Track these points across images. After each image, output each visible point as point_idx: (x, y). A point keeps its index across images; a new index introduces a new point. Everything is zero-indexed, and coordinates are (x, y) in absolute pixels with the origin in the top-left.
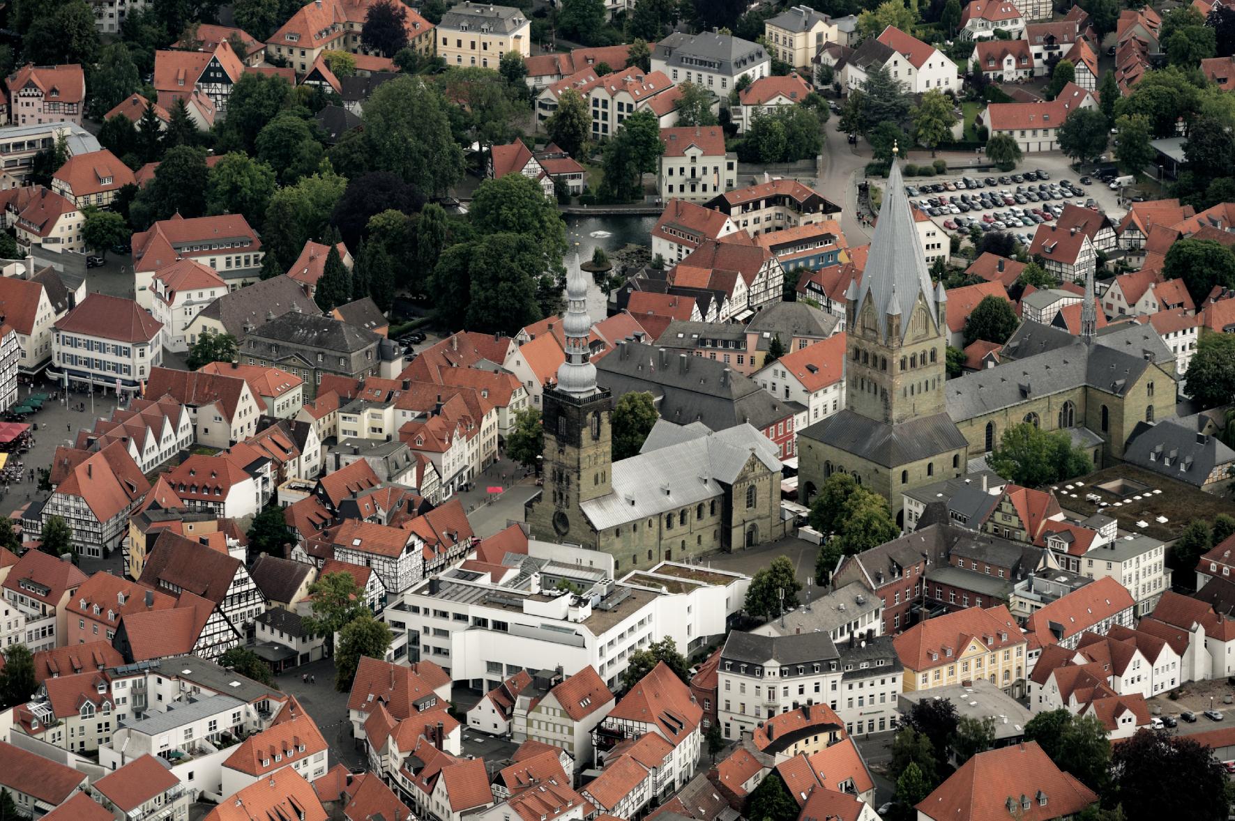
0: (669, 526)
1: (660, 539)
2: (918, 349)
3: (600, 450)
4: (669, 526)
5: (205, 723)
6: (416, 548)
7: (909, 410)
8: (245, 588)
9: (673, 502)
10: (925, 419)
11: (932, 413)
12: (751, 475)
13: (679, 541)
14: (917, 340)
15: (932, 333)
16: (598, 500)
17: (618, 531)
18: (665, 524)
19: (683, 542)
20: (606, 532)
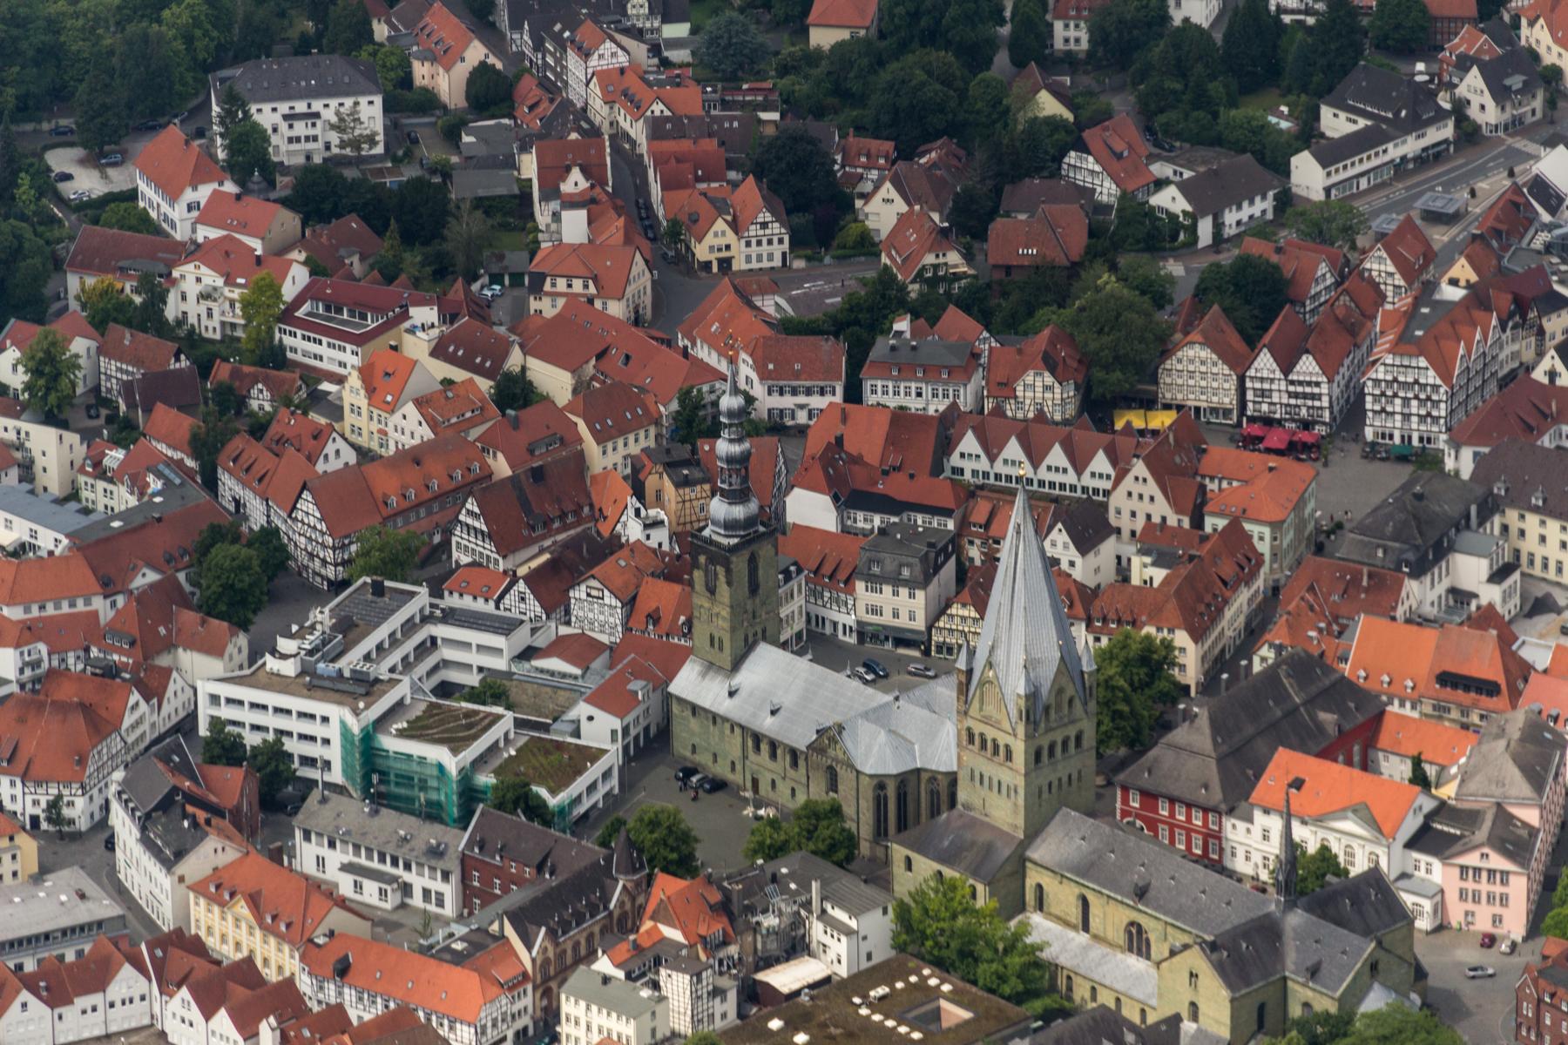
0: (757, 748)
1: (745, 757)
2: (990, 733)
3: (716, 610)
4: (757, 748)
5: (28, 525)
6: (607, 601)
7: (977, 803)
8: (477, 524)
9: (767, 725)
10: (994, 828)
11: (1006, 828)
12: (831, 752)
13: (768, 777)
14: (986, 721)
15: (1007, 727)
16: (710, 667)
17: (695, 709)
18: (750, 743)
19: (773, 782)
20: (680, 700)
